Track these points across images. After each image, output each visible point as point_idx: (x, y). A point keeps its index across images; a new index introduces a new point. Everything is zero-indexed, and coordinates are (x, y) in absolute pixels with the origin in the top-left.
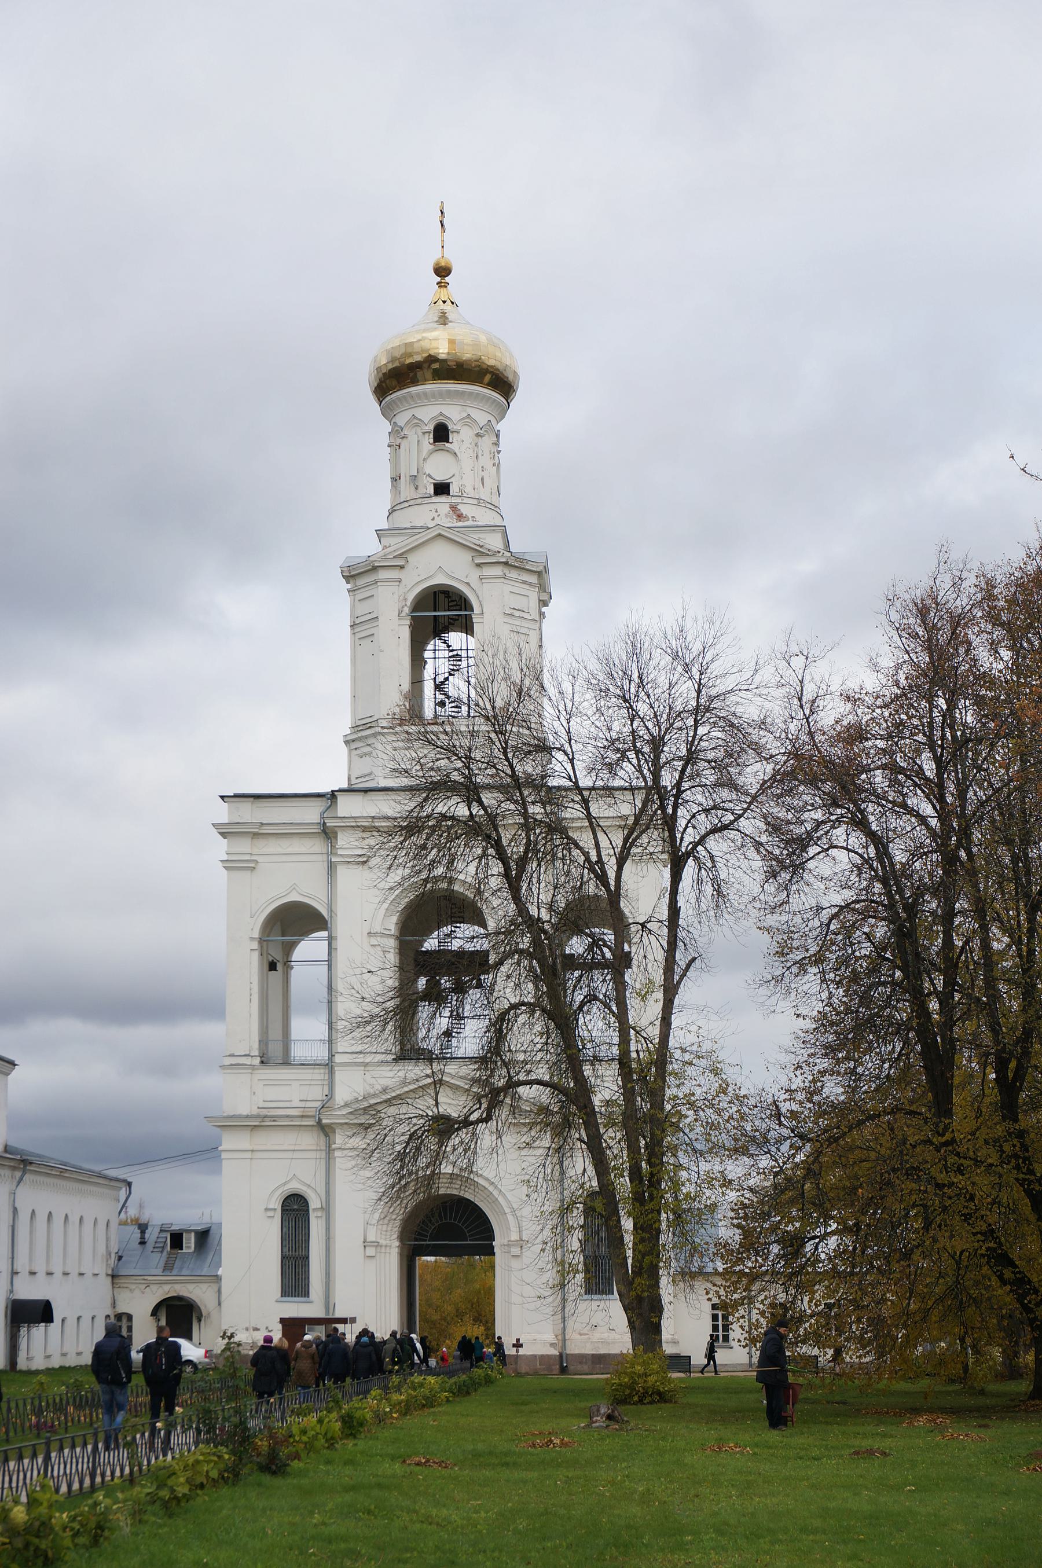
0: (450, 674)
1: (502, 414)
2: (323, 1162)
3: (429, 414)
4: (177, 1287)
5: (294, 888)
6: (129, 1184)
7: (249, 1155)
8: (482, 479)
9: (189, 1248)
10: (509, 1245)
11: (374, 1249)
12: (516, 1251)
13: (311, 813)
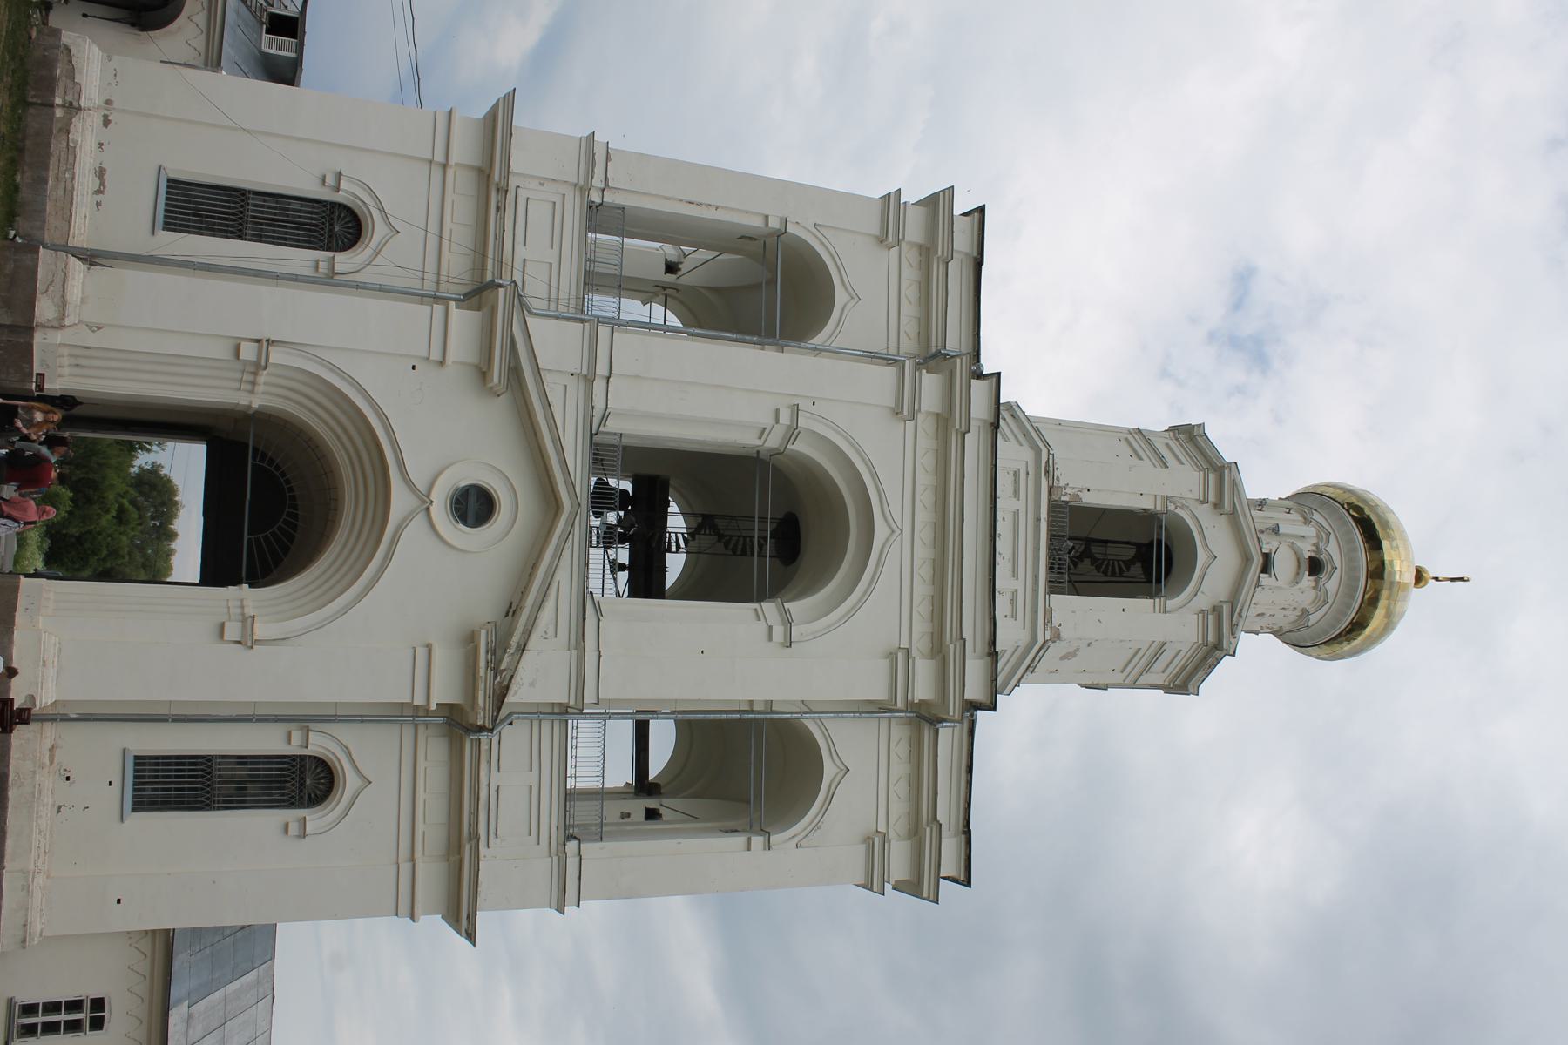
2: (414, 284)
3: (1333, 551)
5: (854, 296)
7: (439, 157)
9: (269, 45)
10: (248, 622)
11: (254, 358)
12: (233, 631)
13: (955, 341)
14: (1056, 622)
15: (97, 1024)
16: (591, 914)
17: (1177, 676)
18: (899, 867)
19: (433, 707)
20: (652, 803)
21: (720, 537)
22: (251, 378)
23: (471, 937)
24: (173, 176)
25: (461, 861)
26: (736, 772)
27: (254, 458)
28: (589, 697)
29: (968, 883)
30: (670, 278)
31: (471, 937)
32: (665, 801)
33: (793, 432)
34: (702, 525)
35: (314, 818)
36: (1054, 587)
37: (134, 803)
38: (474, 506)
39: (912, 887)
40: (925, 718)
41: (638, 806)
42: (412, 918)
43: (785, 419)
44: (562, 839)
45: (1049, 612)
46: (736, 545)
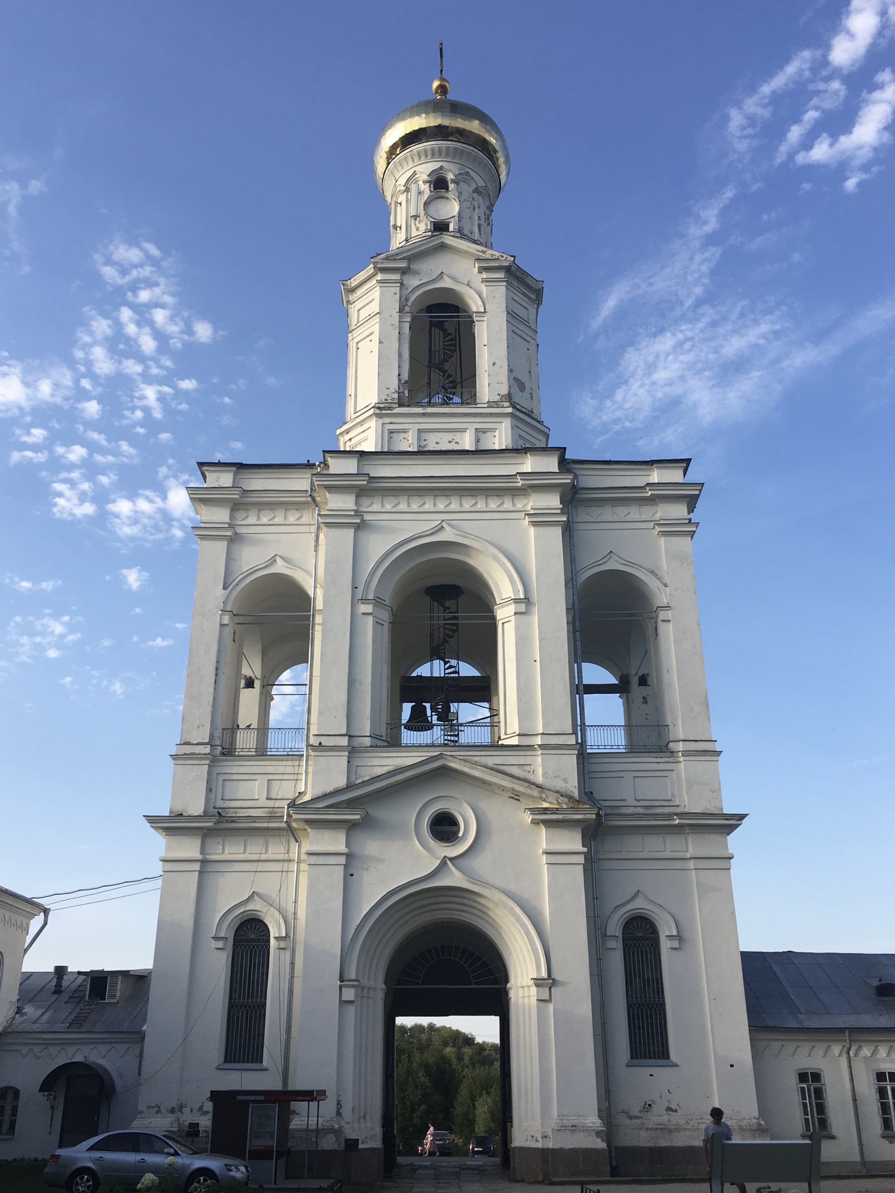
6: (46, 911)
8: (479, 226)
11: (353, 990)
14: (497, 398)
15: (816, 1077)
16: (721, 734)
17: (530, 298)
18: (679, 511)
19: (585, 850)
20: (635, 681)
21: (445, 641)
22: (366, 991)
23: (742, 817)
25: (689, 825)
26: (611, 624)
27: (418, 984)
28: (572, 740)
29: (688, 461)
30: (257, 684)
31: (742, 817)
32: (633, 672)
34: (437, 653)
35: (666, 929)
36: (471, 398)
37: (664, 1058)
38: (444, 827)
39: (692, 502)
40: (573, 498)
41: (638, 692)
42: (731, 858)
43: (369, 608)
44: (668, 754)
45: (491, 404)
46: (450, 630)
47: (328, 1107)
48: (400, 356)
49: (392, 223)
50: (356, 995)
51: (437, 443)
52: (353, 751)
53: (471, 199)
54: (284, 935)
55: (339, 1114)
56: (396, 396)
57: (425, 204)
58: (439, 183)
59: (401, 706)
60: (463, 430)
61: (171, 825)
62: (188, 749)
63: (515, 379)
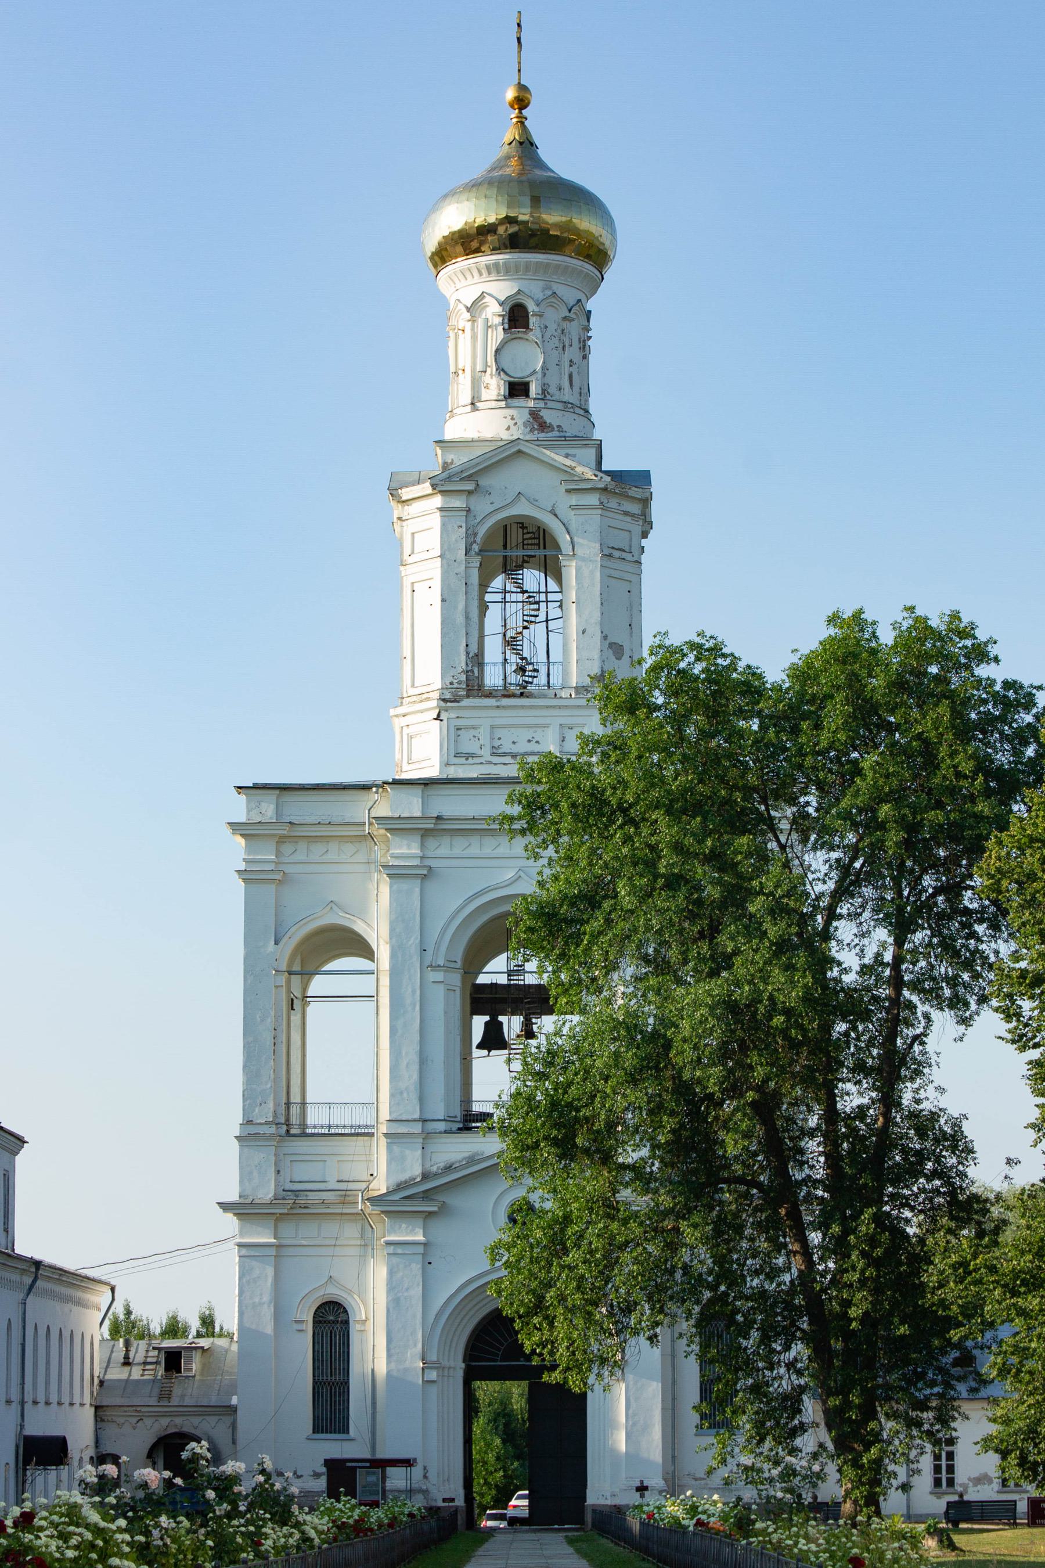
0: (525, 628)
1: (594, 286)
4: (178, 1421)
6: (113, 1290)
8: (571, 376)
24: (311, 1431)
27: (496, 1361)
33: (447, 969)
43: (439, 976)
47: (417, 1471)
48: (467, 618)
49: (452, 369)
50: (438, 1376)
51: (514, 743)
52: (427, 1136)
53: (559, 331)
54: (364, 1318)
55: (425, 1477)
56: (463, 677)
57: (497, 351)
58: (516, 317)
59: (472, 1018)
60: (546, 726)
61: (243, 1210)
62: (252, 1129)
63: (611, 645)
